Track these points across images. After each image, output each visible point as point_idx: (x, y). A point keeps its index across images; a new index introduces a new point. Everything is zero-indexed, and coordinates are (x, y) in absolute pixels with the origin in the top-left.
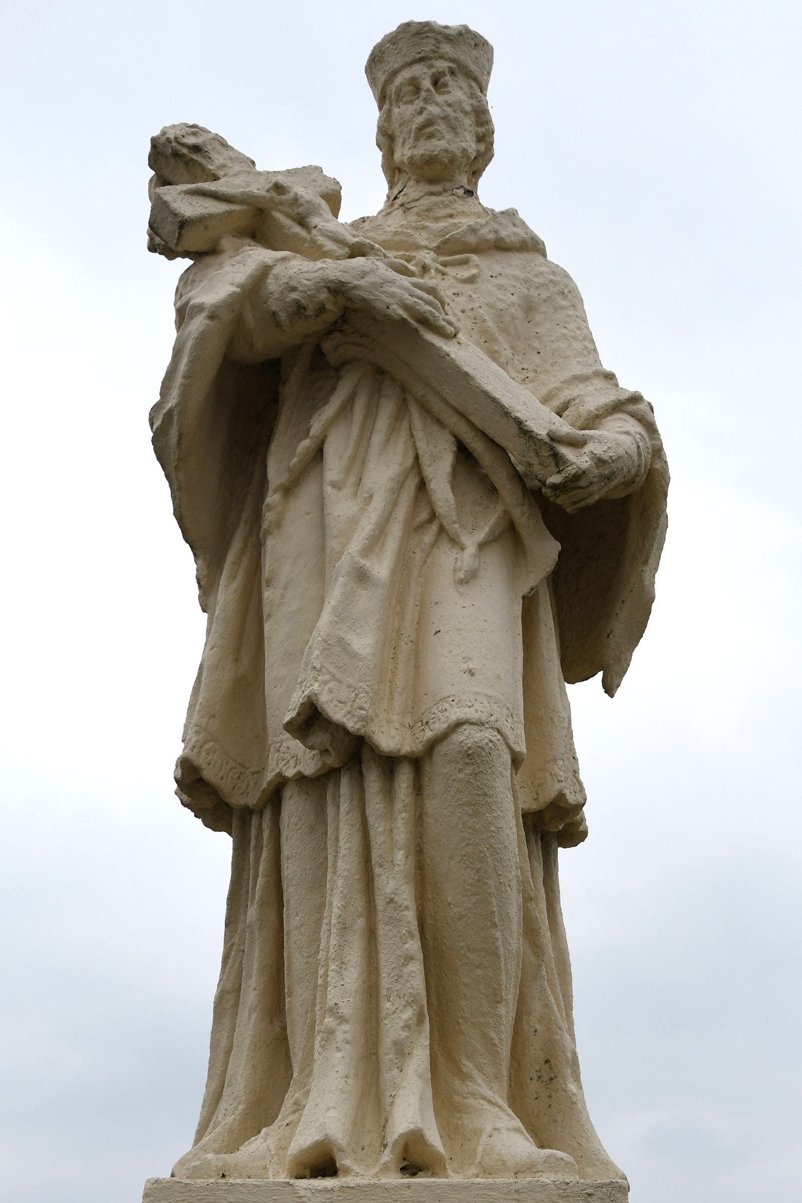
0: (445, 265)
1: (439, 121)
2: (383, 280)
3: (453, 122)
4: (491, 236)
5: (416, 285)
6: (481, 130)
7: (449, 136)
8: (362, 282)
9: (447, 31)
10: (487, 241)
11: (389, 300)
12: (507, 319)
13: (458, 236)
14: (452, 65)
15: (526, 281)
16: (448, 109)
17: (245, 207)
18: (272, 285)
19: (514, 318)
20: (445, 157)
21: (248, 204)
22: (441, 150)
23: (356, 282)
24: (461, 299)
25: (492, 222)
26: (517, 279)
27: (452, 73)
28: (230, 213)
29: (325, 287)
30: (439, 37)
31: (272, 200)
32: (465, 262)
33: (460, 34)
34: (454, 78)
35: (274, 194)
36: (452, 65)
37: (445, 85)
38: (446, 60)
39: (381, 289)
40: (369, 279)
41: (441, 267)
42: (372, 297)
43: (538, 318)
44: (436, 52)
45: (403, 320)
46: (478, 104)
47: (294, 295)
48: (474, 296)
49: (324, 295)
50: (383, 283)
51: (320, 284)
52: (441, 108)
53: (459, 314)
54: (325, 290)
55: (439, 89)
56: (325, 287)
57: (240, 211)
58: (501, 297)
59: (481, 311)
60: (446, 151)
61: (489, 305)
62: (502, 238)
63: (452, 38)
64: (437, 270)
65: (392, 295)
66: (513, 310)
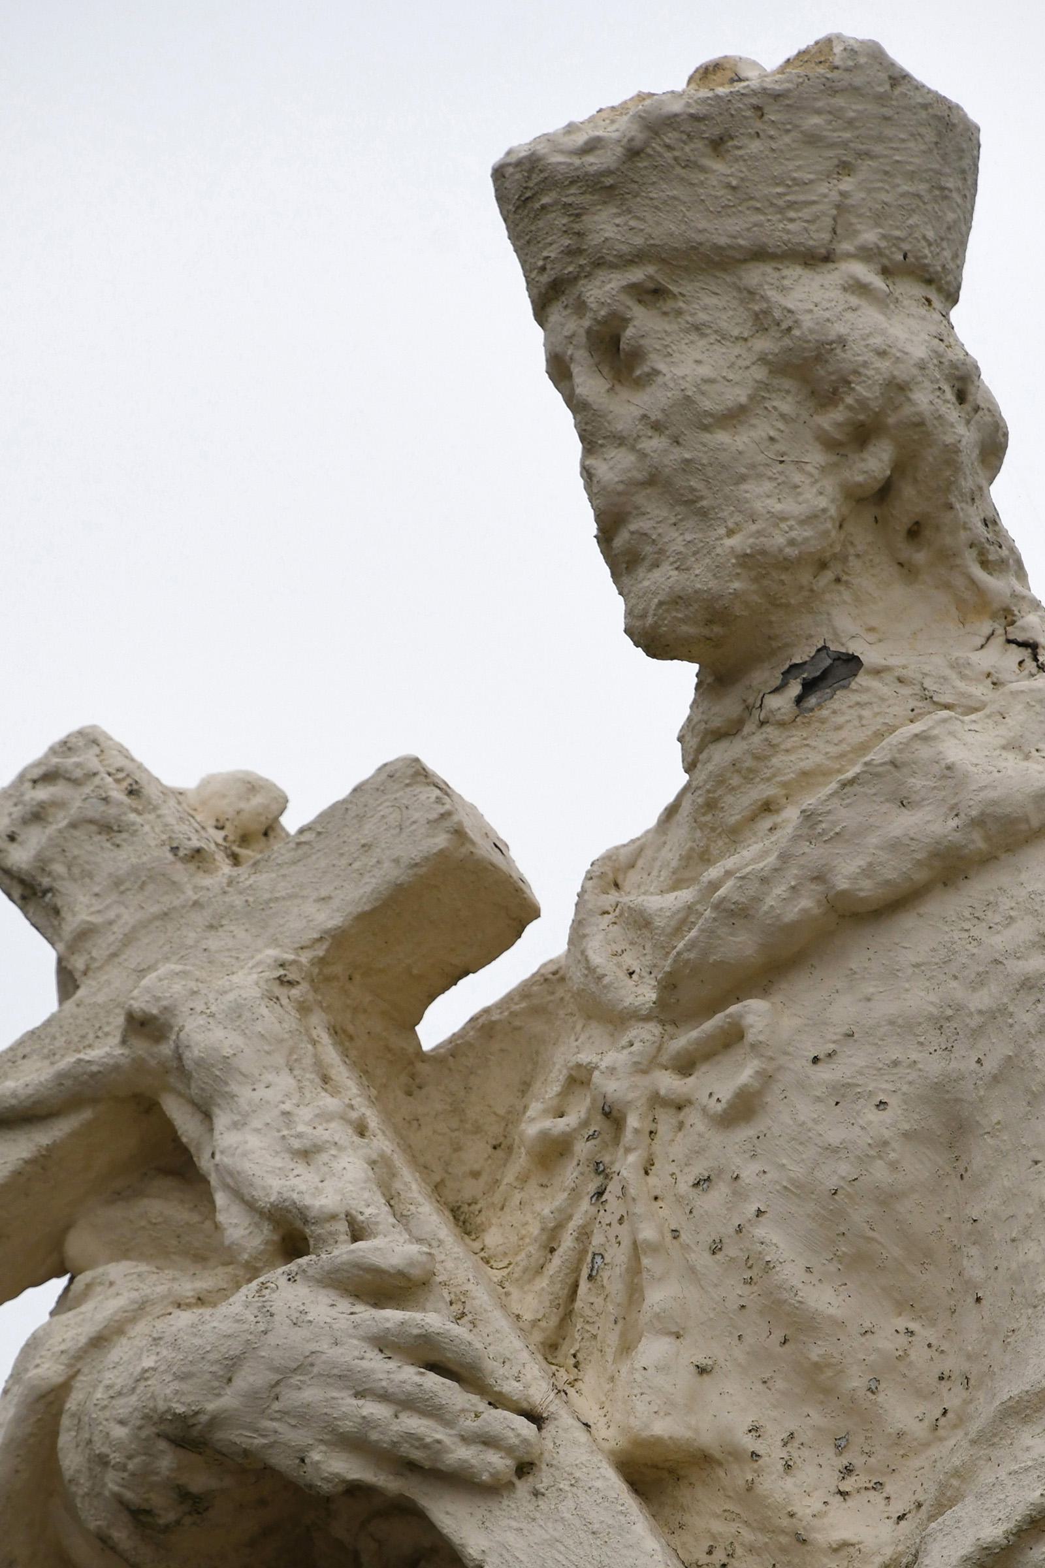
0: (685, 1066)
1: (640, 499)
2: (276, 1370)
3: (680, 482)
4: (806, 903)
5: (384, 1343)
6: (832, 419)
7: (676, 540)
8: (228, 1400)
9: (595, 162)
10: (791, 929)
11: (297, 1437)
12: (860, 1215)
13: (692, 956)
14: (637, 275)
15: (939, 1023)
16: (654, 444)
17: (87, 1114)
18: (71, 1460)
19: (886, 1199)
20: (683, 621)
21: (94, 1101)
22: (661, 604)
23: (211, 1406)
24: (719, 1193)
25: (805, 847)
26: (904, 1027)
27: (652, 294)
28: (42, 1162)
29: (158, 1435)
30: (573, 196)
31: (139, 1065)
32: (733, 1037)
33: (633, 153)
34: (669, 305)
35: (141, 1047)
36: (637, 275)
37: (637, 355)
38: (613, 266)
39: (276, 1406)
40: (249, 1378)
41: (668, 1082)
42: (261, 1441)
43: (978, 1158)
44: (579, 252)
45: (354, 1490)
46: (787, 342)
47: (112, 1482)
48: (749, 1172)
49: (166, 1462)
50: (278, 1383)
51: (144, 1434)
52: (633, 448)
53: (702, 1259)
54: (162, 1445)
55: (631, 369)
56: (158, 1435)
57: (74, 1134)
58: (834, 1136)
59: (761, 1231)
60: (677, 600)
61: (797, 1190)
62: (843, 893)
63: (609, 181)
64: (657, 1101)
65: (302, 1417)
66: (879, 1172)
